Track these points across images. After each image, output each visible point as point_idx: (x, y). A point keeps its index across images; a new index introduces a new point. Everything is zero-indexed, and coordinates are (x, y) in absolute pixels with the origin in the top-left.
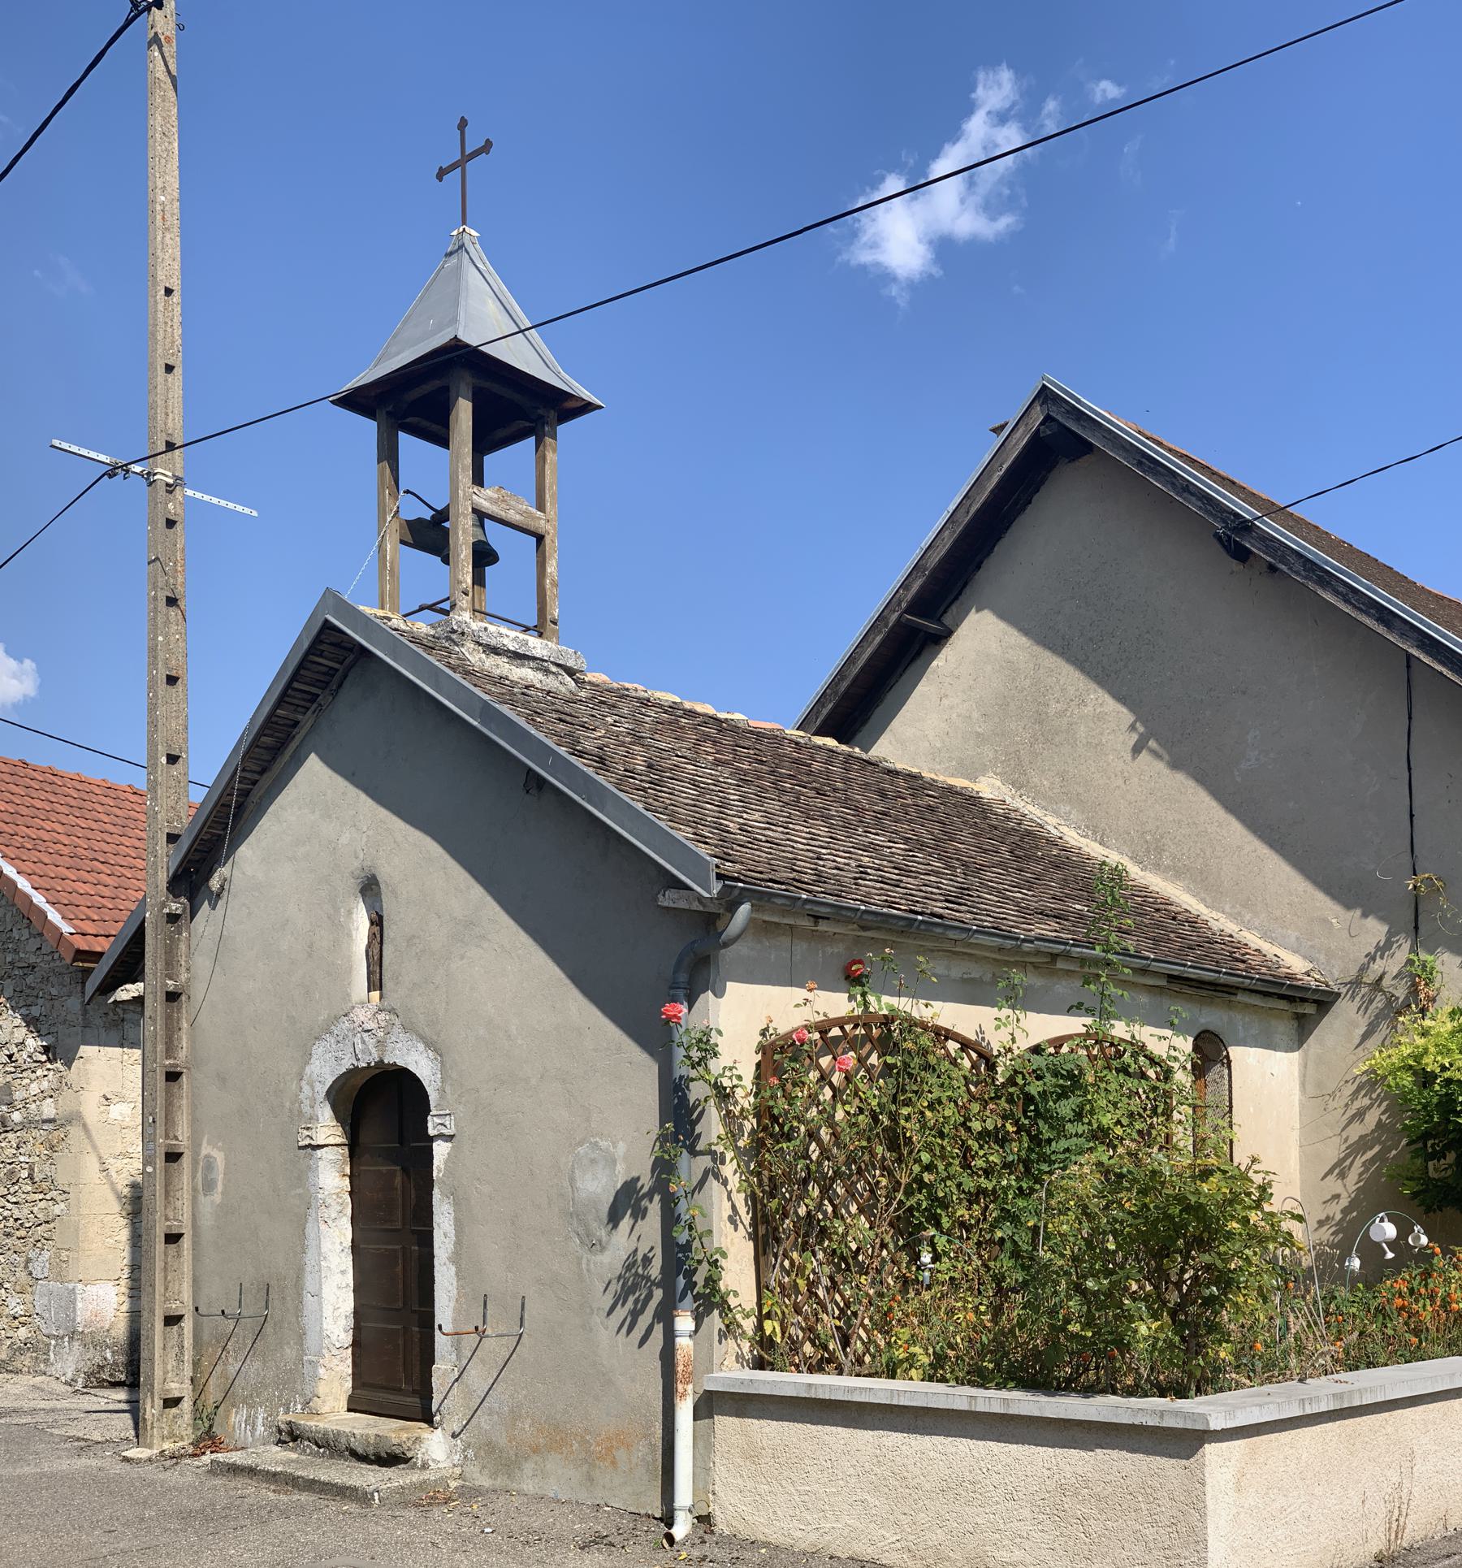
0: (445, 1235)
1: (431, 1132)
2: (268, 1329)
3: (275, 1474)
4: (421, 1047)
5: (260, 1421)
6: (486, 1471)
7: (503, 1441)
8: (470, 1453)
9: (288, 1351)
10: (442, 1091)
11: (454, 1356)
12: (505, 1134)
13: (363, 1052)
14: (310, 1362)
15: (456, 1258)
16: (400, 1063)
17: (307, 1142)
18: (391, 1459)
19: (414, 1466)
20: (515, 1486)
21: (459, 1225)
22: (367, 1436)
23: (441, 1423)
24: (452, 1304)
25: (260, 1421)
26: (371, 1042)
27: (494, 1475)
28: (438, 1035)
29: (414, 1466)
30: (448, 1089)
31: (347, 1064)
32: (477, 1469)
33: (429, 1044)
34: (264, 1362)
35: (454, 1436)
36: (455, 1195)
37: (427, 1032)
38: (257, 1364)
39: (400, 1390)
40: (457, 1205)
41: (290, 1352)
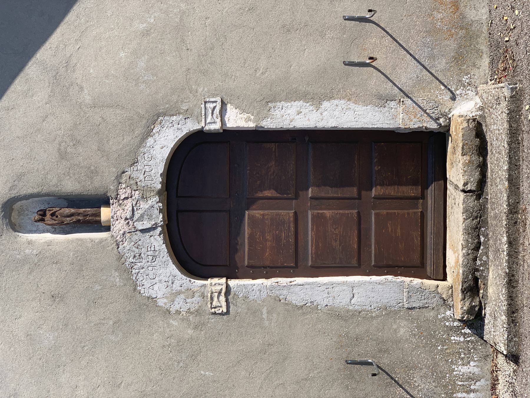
0: (299, 113)
1: (216, 126)
2: (385, 361)
3: (510, 243)
4: (150, 141)
5: (464, 369)
6: (478, 62)
7: (452, 44)
8: (465, 79)
9: (402, 331)
10: (188, 115)
11: (393, 104)
12: (222, 39)
13: (150, 218)
14: (409, 297)
15: (316, 99)
16: (161, 168)
17: (223, 298)
18: (478, 132)
19: (483, 117)
20: (485, 29)
21: (293, 96)
22: (464, 165)
23: (445, 115)
24: (352, 105)
25: (464, 369)
26: (144, 206)
27: (479, 54)
28: (141, 117)
29: (483, 117)
30: (184, 107)
31: (157, 242)
32: (475, 71)
33: (148, 133)
34: (415, 367)
35: (453, 98)
36: (269, 100)
37: (138, 131)
38: (417, 380)
39: (422, 212)
40: (274, 100)
41: (403, 329)
